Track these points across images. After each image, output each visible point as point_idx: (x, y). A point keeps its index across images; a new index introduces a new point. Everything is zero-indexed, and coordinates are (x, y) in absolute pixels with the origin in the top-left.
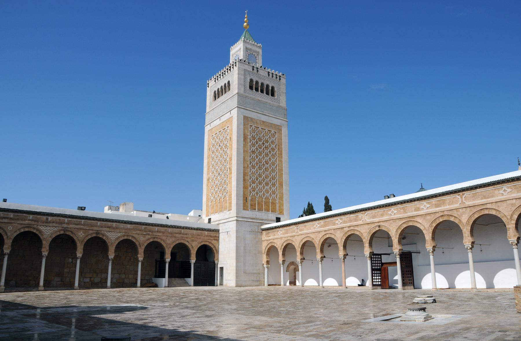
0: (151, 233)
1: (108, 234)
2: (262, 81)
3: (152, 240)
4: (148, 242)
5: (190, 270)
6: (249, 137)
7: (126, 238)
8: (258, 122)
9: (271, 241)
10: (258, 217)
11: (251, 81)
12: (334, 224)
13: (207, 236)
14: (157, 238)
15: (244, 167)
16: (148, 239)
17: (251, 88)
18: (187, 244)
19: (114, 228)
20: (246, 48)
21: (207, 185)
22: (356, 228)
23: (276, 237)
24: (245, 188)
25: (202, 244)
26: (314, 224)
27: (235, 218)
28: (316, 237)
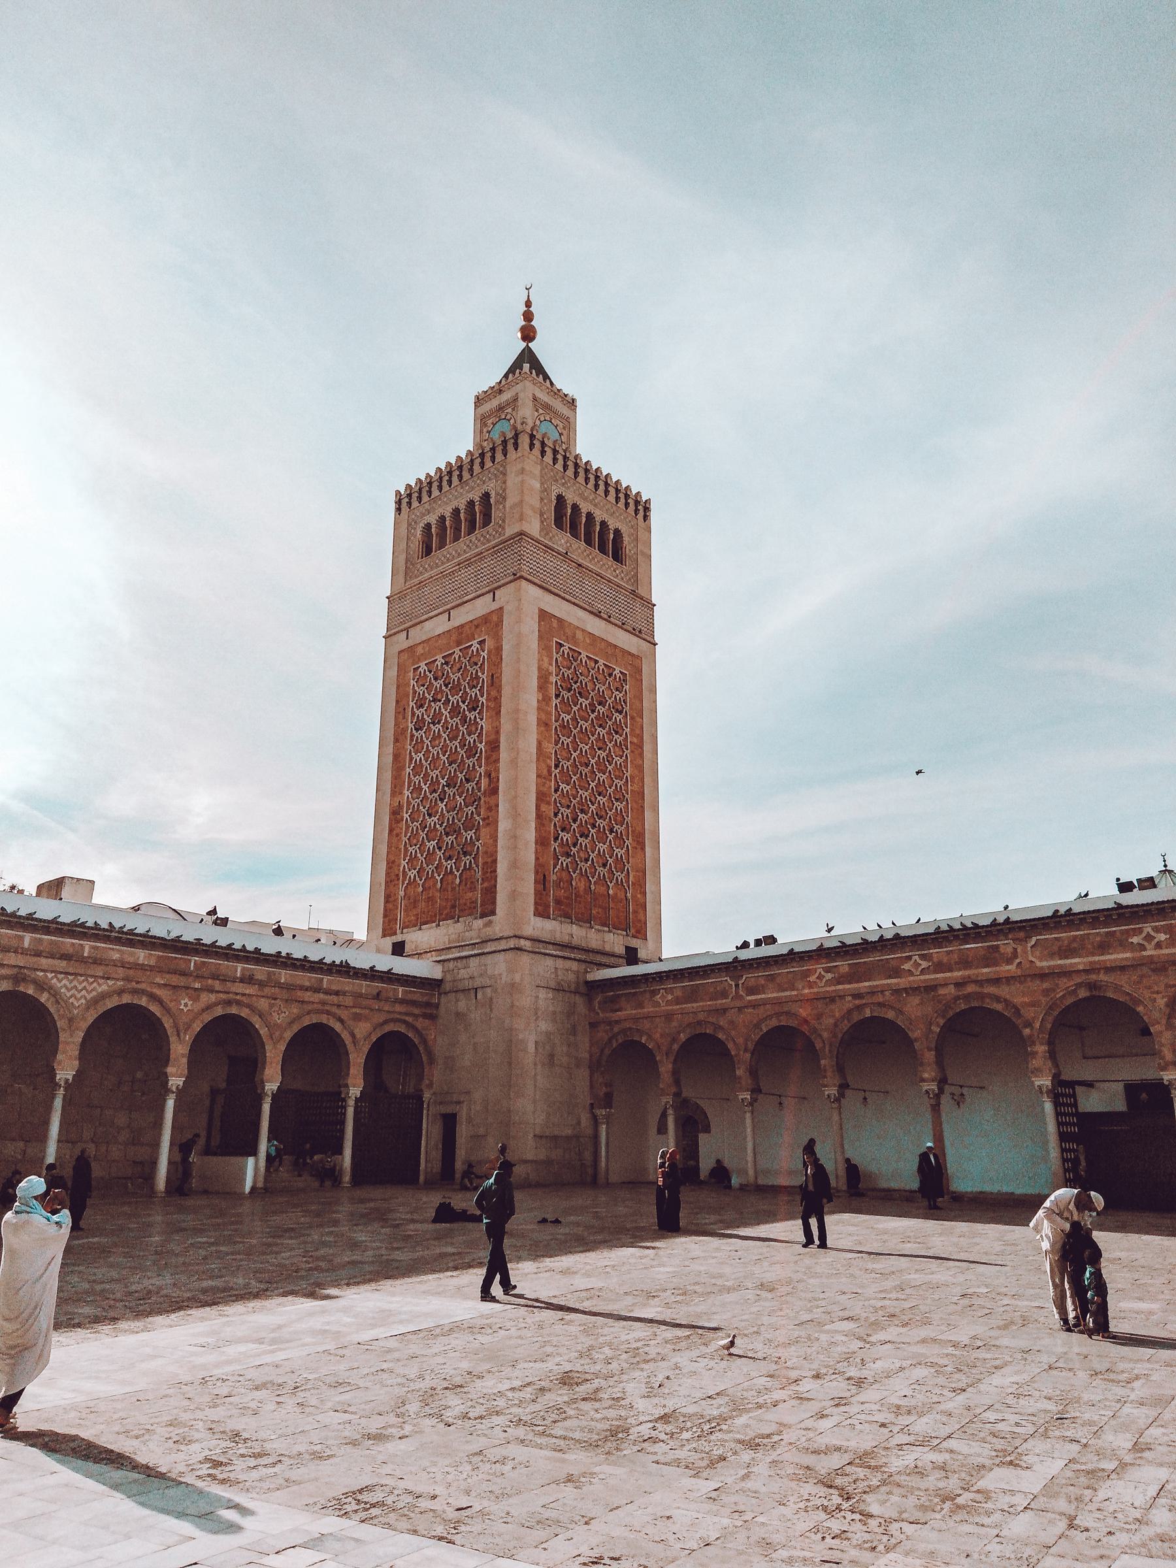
0: (217, 985)
1: (61, 984)
2: (591, 508)
3: (219, 1011)
4: (207, 1018)
5: (343, 1122)
6: (553, 679)
7: (126, 999)
8: (579, 635)
9: (627, 1025)
10: (575, 941)
11: (560, 499)
12: (896, 972)
13: (402, 1002)
14: (238, 1003)
15: (538, 776)
16: (208, 1008)
17: (559, 523)
18: (337, 1027)
19: (83, 960)
20: (535, 399)
21: (391, 831)
22: (992, 990)
23: (649, 1009)
24: (542, 842)
25: (388, 1028)
26: (807, 974)
27: (512, 943)
28: (819, 1017)
